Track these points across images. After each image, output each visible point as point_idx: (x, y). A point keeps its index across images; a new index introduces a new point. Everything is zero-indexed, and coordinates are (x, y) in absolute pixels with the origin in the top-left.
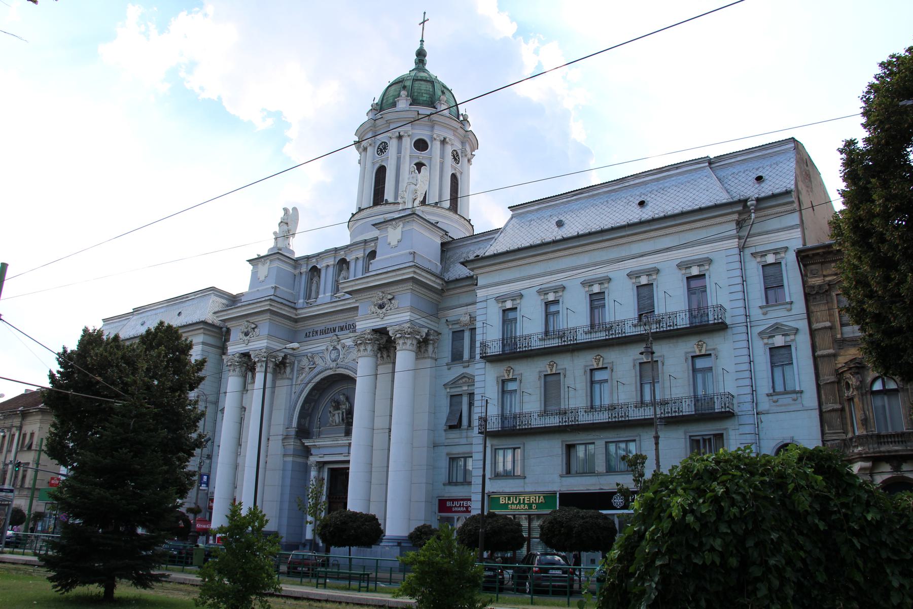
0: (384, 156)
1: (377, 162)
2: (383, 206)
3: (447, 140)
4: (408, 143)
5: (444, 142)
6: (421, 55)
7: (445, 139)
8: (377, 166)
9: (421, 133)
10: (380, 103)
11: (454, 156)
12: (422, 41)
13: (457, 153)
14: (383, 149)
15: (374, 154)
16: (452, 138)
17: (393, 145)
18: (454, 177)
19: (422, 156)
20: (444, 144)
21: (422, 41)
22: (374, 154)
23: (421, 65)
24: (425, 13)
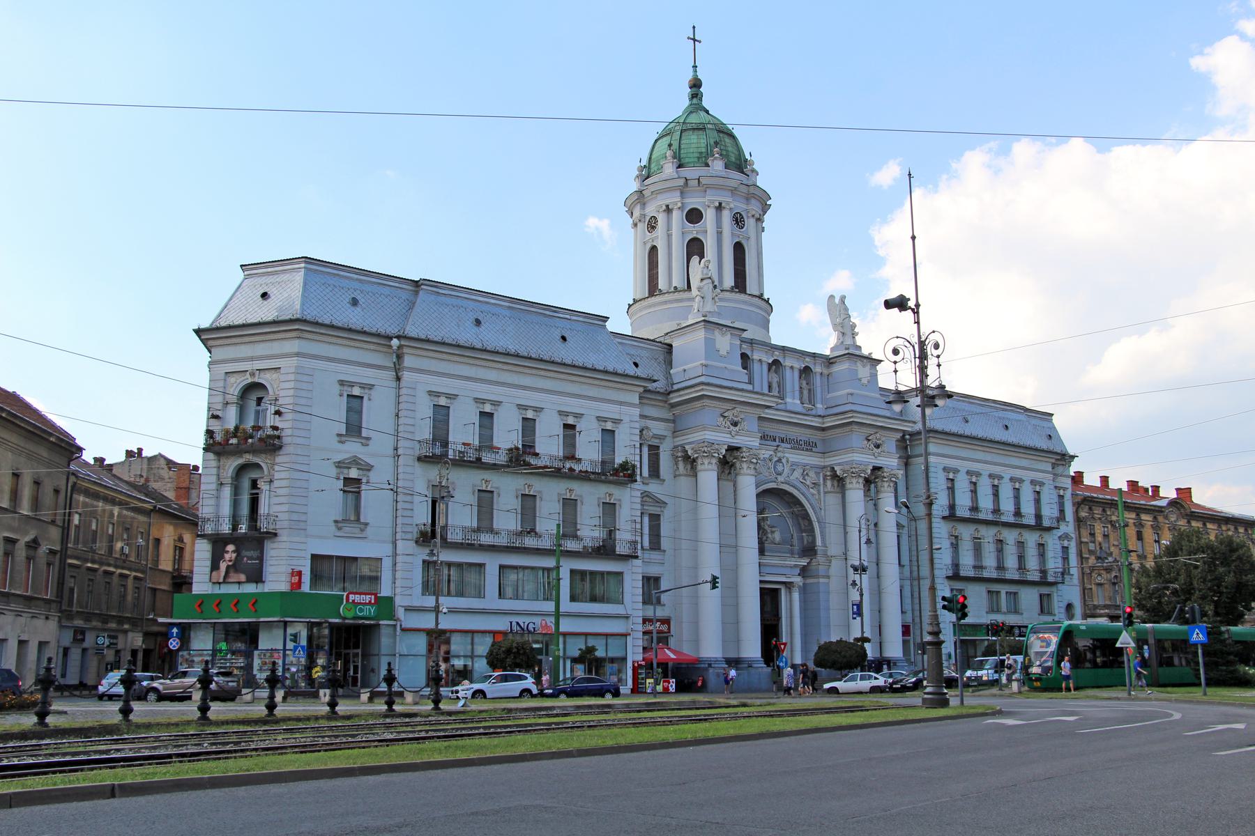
0: (654, 234)
1: (648, 241)
2: (657, 297)
3: (723, 205)
4: (677, 217)
5: (720, 208)
6: (696, 84)
9: (693, 202)
10: (647, 165)
11: (737, 219)
12: (695, 67)
13: (741, 215)
14: (652, 226)
15: (644, 231)
16: (730, 200)
17: (661, 218)
18: (739, 249)
19: (693, 230)
20: (721, 210)
21: (695, 67)
22: (644, 231)
23: (695, 101)
24: (694, 27)
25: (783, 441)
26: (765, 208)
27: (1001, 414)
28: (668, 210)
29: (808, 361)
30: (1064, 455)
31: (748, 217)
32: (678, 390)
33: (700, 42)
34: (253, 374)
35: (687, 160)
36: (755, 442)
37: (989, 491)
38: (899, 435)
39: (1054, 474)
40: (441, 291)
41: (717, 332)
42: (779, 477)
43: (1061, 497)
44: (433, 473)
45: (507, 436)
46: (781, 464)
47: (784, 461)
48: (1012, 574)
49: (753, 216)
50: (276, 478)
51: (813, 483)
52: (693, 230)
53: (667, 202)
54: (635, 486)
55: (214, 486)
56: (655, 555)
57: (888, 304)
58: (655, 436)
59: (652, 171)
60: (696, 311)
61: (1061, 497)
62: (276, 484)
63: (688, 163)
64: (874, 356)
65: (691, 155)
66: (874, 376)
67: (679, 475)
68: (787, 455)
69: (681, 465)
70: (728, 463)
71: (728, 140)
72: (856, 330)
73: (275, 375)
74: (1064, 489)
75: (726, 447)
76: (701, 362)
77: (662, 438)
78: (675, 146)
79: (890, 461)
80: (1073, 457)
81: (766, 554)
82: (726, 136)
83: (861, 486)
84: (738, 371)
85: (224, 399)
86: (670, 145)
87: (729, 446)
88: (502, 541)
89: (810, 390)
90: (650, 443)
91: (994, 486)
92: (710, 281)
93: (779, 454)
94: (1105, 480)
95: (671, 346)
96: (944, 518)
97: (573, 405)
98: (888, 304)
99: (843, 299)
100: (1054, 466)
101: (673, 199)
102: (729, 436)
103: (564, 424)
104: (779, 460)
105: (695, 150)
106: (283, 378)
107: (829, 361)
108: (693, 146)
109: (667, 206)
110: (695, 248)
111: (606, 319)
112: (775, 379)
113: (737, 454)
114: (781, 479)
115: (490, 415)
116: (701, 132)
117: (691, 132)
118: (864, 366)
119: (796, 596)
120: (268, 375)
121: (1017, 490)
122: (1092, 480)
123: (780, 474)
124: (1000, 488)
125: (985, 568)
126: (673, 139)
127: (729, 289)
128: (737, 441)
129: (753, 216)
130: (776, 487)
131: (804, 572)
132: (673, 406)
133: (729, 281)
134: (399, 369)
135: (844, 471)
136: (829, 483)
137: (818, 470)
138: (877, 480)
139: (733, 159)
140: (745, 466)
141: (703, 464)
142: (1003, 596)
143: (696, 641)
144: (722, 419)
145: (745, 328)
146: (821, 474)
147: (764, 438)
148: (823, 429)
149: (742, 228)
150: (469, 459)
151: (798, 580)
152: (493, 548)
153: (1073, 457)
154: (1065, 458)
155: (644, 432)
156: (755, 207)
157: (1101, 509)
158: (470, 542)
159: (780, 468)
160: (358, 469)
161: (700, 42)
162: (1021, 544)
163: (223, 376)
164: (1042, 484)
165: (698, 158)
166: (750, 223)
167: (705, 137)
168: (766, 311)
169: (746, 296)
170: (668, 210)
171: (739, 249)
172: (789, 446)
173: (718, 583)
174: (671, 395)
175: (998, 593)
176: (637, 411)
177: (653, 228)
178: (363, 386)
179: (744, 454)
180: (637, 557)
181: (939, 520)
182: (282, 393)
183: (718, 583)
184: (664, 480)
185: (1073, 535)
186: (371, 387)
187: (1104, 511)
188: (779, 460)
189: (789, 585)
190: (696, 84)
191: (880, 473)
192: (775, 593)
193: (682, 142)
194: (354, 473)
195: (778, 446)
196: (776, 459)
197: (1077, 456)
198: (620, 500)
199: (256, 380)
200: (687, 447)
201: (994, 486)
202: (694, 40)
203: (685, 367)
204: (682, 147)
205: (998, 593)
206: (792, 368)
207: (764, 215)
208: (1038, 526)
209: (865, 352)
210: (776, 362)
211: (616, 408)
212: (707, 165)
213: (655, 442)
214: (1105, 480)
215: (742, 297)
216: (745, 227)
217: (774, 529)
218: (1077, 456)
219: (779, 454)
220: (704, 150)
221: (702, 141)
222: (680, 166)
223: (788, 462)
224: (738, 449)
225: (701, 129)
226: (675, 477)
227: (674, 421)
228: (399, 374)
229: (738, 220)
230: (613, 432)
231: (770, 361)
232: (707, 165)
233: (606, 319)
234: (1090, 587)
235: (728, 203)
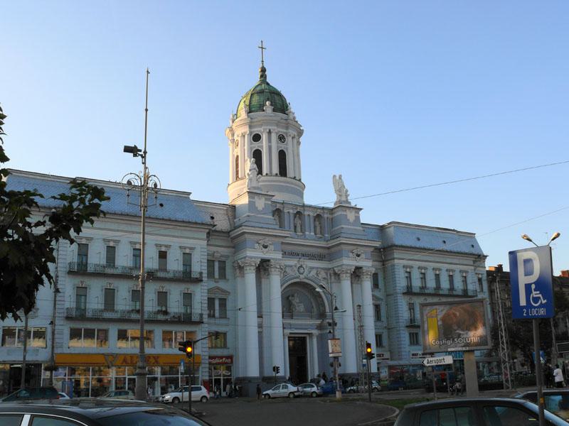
5: (270, 132)
6: (263, 70)
7: (270, 130)
16: (276, 128)
18: (282, 155)
19: (256, 145)
25: (303, 256)
26: (300, 133)
27: (442, 235)
29: (319, 212)
30: (479, 256)
35: (253, 109)
36: (279, 256)
37: (447, 278)
38: (372, 249)
41: (256, 197)
42: (301, 276)
44: (77, 281)
45: (175, 264)
47: (304, 266)
52: (256, 145)
54: (203, 284)
56: (223, 321)
57: (127, 149)
58: (222, 256)
64: (358, 207)
66: (358, 218)
70: (263, 268)
72: (348, 193)
75: (260, 260)
77: (227, 257)
79: (368, 264)
80: (486, 256)
83: (349, 278)
86: (245, 102)
87: (262, 260)
89: (321, 227)
96: (404, 294)
97: (164, 240)
98: (127, 149)
99: (340, 177)
100: (474, 262)
104: (301, 266)
107: (331, 211)
111: (190, 193)
112: (298, 222)
118: (351, 212)
119: (315, 340)
123: (302, 274)
128: (266, 256)
131: (320, 327)
132: (233, 239)
133: (276, 170)
135: (339, 270)
136: (333, 277)
140: (273, 270)
143: (246, 367)
147: (284, 253)
148: (329, 248)
151: (315, 332)
153: (486, 256)
156: (292, 132)
159: (302, 270)
164: (466, 272)
166: (289, 140)
171: (282, 155)
174: (231, 233)
181: (401, 295)
185: (488, 300)
188: (301, 266)
190: (263, 70)
196: (298, 266)
198: (117, 287)
200: (239, 261)
206: (309, 215)
209: (353, 205)
212: (264, 111)
213: (223, 259)
224: (361, 268)
227: (234, 247)
229: (281, 138)
230: (114, 247)
232: (264, 111)
233: (190, 193)
235: (274, 130)
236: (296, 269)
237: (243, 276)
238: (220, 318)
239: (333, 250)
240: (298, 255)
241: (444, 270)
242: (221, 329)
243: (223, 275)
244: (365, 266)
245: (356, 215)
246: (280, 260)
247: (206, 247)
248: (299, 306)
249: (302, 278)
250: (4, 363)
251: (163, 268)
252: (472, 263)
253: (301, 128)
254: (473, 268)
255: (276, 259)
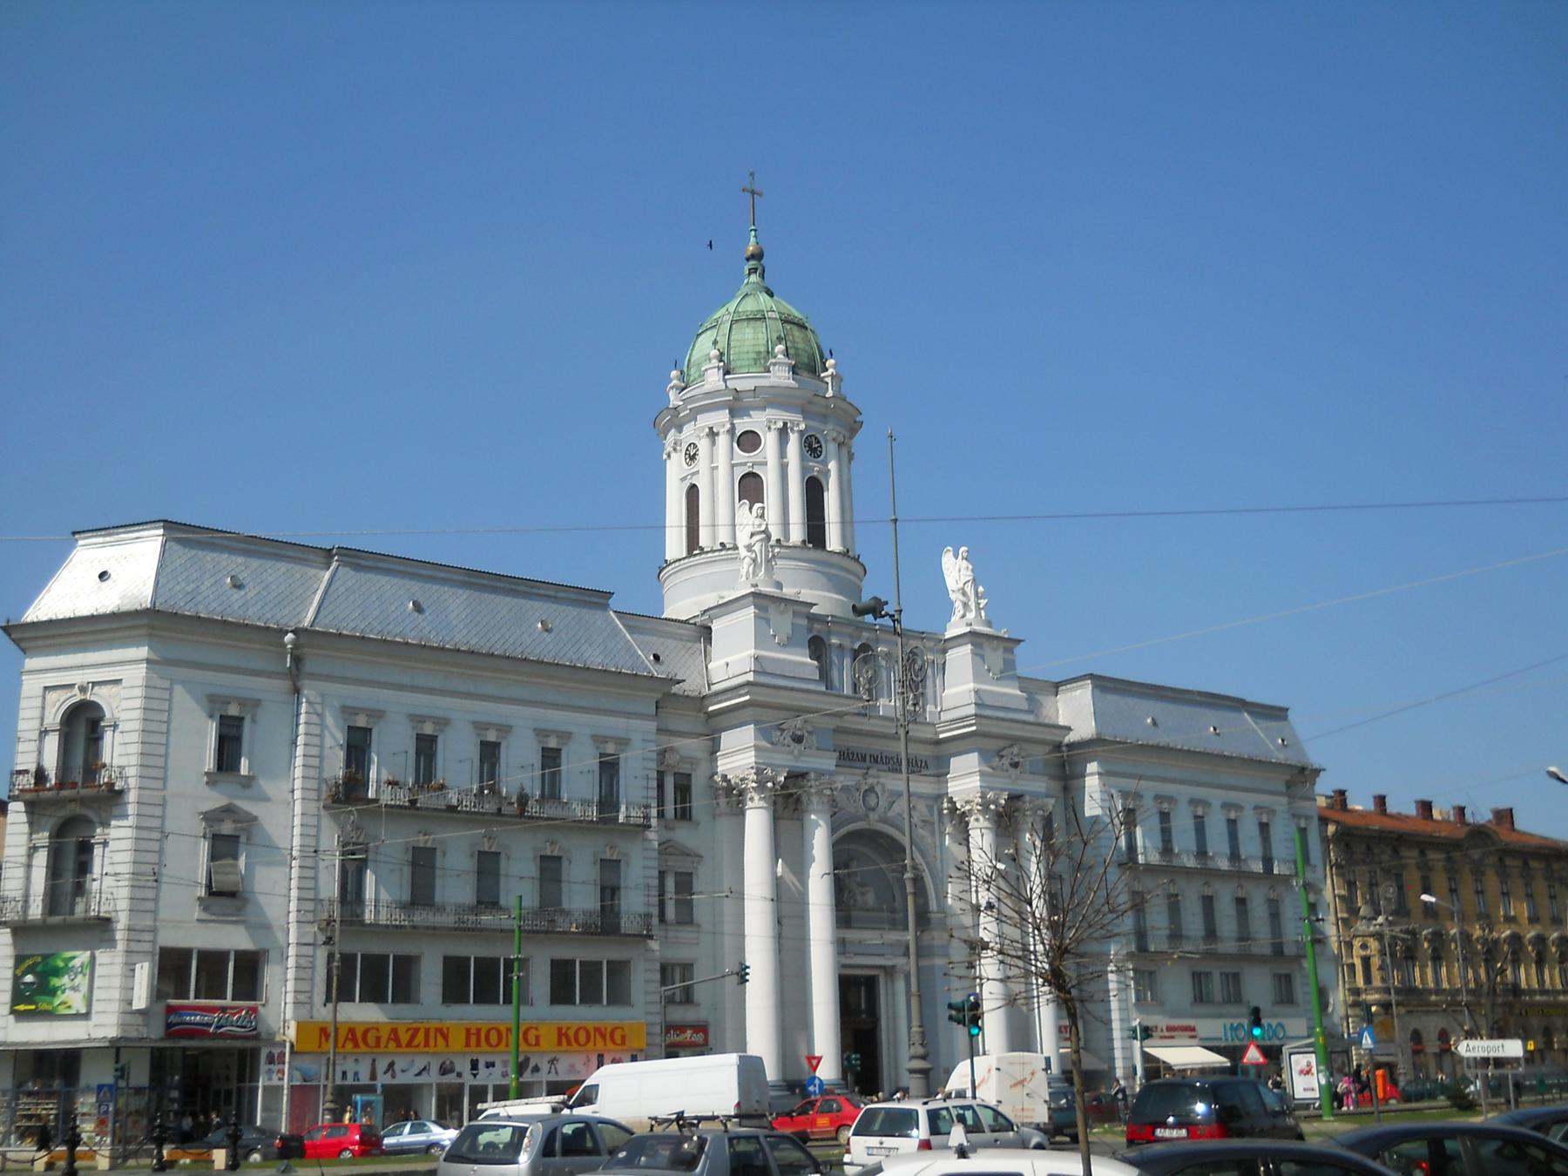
8: (687, 484)
9: (743, 425)
11: (810, 446)
17: (703, 445)
25: (876, 761)
28: (712, 434)
30: (1303, 769)
31: (826, 441)
32: (717, 694)
33: (760, 195)
34: (83, 689)
35: (739, 363)
36: (828, 762)
39: (1289, 797)
40: (363, 562)
43: (1303, 832)
46: (873, 795)
47: (878, 789)
48: (1228, 946)
49: (834, 440)
50: (111, 837)
51: (923, 821)
53: (710, 423)
55: (23, 851)
59: (692, 378)
60: (744, 578)
61: (1303, 832)
62: (112, 845)
63: (741, 367)
65: (745, 356)
67: (720, 815)
68: (881, 780)
69: (722, 800)
71: (797, 333)
73: (114, 689)
74: (1307, 818)
76: (749, 652)
78: (722, 344)
80: (1317, 772)
81: (853, 925)
82: (795, 328)
84: (803, 664)
85: (42, 725)
86: (715, 343)
88: (447, 920)
90: (676, 770)
91: (1196, 817)
92: (763, 536)
93: (871, 781)
94: (1381, 801)
95: (710, 628)
100: (1289, 785)
101: (720, 418)
102: (789, 757)
103: (543, 748)
104: (871, 789)
105: (751, 349)
106: (125, 693)
108: (747, 343)
109: (711, 429)
110: (750, 487)
113: (801, 782)
114: (873, 816)
115: (432, 740)
116: (758, 323)
117: (745, 324)
119: (900, 985)
120: (104, 690)
121: (1232, 823)
122: (1360, 803)
123: (873, 809)
124: (1206, 819)
125: (1188, 938)
126: (721, 333)
127: (799, 544)
129: (834, 440)
130: (867, 827)
133: (797, 534)
134: (297, 676)
137: (930, 803)
138: (1016, 814)
139: (806, 360)
140: (815, 799)
141: (752, 799)
142: (1216, 978)
144: (779, 733)
145: (814, 602)
146: (935, 808)
149: (819, 456)
150: (398, 803)
152: (433, 931)
153: (1317, 772)
154: (1303, 775)
155: (667, 755)
157: (1364, 846)
158: (397, 923)
159: (872, 801)
160: (234, 821)
161: (760, 195)
162: (1208, 902)
163: (40, 692)
164: (1272, 812)
165: (755, 360)
167: (764, 330)
168: (855, 574)
169: (824, 554)
170: (712, 434)
172: (886, 767)
173: (748, 974)
175: (1208, 974)
176: (652, 726)
177: (693, 458)
178: (243, 702)
179: (813, 783)
180: (651, 937)
182: (123, 716)
183: (748, 974)
184: (698, 824)
186: (257, 703)
187: (1369, 848)
188: (871, 789)
189: (890, 971)
191: (1020, 803)
192: (870, 983)
193: (732, 338)
194: (227, 828)
195: (868, 769)
197: (1324, 770)
199: (88, 697)
201: (1196, 817)
202: (753, 193)
203: (728, 660)
204: (732, 344)
205: (1208, 974)
207: (851, 438)
208: (1240, 875)
210: (865, 647)
211: (620, 722)
213: (685, 768)
214: (1381, 801)
215: (818, 554)
216: (822, 457)
217: (864, 889)
218: (1324, 770)
219: (871, 781)
220: (763, 349)
221: (760, 336)
222: (727, 372)
223: (884, 791)
225: (760, 319)
226: (714, 818)
228: (299, 683)
231: (856, 647)
234: (1350, 961)
236: (859, 796)
237: (739, 813)
238: (679, 923)
239: (944, 747)
240: (864, 759)
241: (1216, 804)
242: (681, 954)
243: (684, 814)
244: (1032, 794)
245: (1009, 656)
246: (831, 774)
247: (653, 737)
248: (863, 894)
249: (874, 822)
250: (3, 1044)
251: (551, 791)
252: (1283, 789)
253: (859, 419)
254: (1285, 800)
255: (821, 774)
